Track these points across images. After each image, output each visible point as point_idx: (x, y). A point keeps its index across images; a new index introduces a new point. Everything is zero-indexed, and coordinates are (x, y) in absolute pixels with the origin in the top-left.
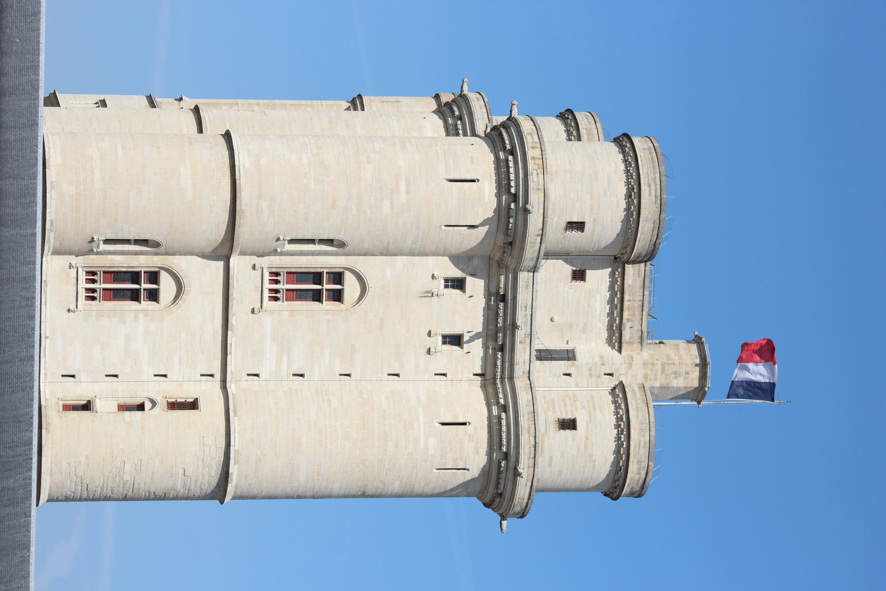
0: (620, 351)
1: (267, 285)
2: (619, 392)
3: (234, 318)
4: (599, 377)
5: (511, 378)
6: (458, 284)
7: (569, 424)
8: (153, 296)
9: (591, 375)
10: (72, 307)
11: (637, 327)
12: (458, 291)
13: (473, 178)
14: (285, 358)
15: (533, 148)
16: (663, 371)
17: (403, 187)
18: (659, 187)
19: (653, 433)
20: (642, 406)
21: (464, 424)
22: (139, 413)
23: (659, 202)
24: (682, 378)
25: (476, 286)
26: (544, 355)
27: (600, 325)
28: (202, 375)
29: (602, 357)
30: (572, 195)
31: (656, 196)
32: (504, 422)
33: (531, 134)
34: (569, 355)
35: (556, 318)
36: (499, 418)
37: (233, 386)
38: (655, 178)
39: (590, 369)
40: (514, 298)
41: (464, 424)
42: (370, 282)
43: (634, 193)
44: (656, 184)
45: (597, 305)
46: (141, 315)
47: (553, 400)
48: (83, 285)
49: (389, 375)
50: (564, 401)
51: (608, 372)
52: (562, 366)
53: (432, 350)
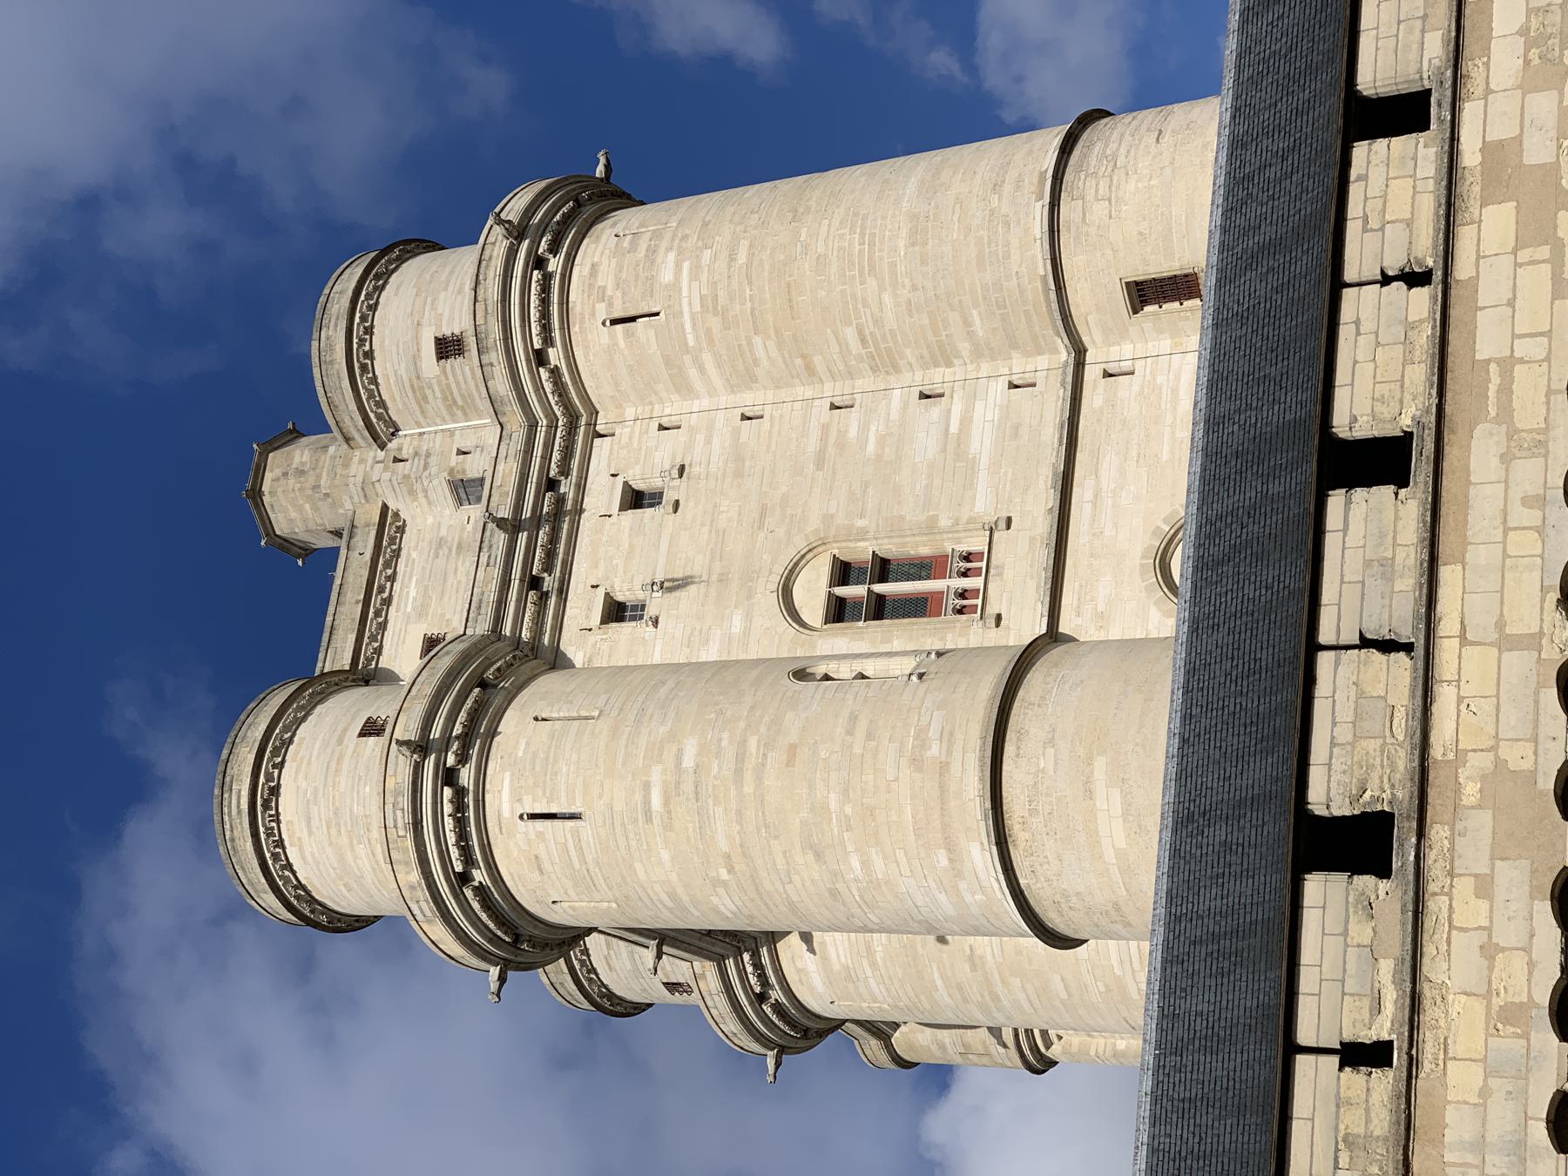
0: (385, 508)
2: (381, 430)
4: (416, 454)
5: (533, 426)
6: (616, 612)
7: (447, 348)
9: (428, 455)
11: (354, 555)
12: (620, 598)
14: (954, 428)
15: (412, 888)
18: (226, 810)
19: (315, 344)
20: (336, 399)
21: (614, 322)
23: (228, 779)
25: (583, 608)
27: (414, 555)
29: (412, 492)
37: (1064, 356)
39: (426, 467)
41: (614, 322)
42: (769, 600)
43: (265, 799)
45: (413, 593)
52: (475, 467)
53: (675, 473)
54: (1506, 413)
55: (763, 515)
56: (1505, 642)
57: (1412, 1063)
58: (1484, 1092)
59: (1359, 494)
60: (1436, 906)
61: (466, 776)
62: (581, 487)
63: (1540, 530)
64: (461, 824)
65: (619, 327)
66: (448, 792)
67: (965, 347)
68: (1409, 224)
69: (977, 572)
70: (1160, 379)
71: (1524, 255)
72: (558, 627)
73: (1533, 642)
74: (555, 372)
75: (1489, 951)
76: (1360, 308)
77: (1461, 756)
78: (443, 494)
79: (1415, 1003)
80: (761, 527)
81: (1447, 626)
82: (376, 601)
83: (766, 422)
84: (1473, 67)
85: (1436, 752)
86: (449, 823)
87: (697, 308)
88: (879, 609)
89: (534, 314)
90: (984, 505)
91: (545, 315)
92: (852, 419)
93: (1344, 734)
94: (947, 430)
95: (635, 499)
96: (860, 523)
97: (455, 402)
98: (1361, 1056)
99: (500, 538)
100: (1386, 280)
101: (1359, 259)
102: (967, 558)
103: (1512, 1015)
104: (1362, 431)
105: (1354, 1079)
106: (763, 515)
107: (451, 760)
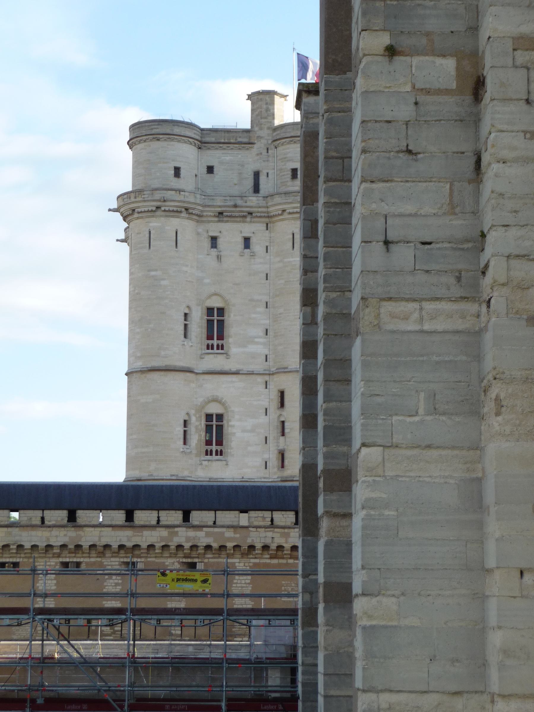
1: (215, 351)
3: (232, 370)
4: (268, 156)
8: (220, 417)
9: (268, 161)
10: (224, 463)
12: (218, 240)
13: (148, 232)
14: (256, 340)
15: (130, 198)
16: (266, 118)
18: (153, 123)
21: (293, 234)
22: (286, 424)
23: (161, 123)
24: (270, 107)
26: (256, 189)
27: (240, 156)
28: (266, 388)
29: (258, 155)
30: (158, 174)
31: (158, 125)
32: (291, 211)
33: (123, 200)
34: (257, 175)
35: (236, 182)
36: (290, 213)
37: (272, 370)
38: (149, 126)
40: (220, 207)
41: (293, 234)
44: (152, 125)
45: (228, 158)
46: (230, 423)
47: (281, 183)
48: (214, 457)
49: (267, 279)
50: (281, 176)
51: (266, 151)
52: (263, 179)
53: (252, 254)
54: (135, 536)
55: (237, 284)
56: (100, 537)
57: (41, 527)
59: (125, 515)
60: (63, 529)
61: (159, 213)
63: (116, 541)
65: (291, 236)
66: (154, 209)
68: (167, 520)
69: (218, 349)
70: (263, 396)
71: (159, 538)
72: (209, 222)
73: (100, 540)
75: (57, 536)
76: (154, 514)
77: (84, 531)
78: (256, 166)
79: (49, 527)
80: (234, 284)
81: (103, 529)
82: (225, 146)
83: (265, 281)
84: (191, 529)
86: (146, 209)
88: (210, 323)
90: (234, 350)
92: (262, 309)
93: (88, 515)
94: (256, 338)
96: (232, 315)
97: (281, 173)
98: (43, 519)
99: (232, 203)
100: (158, 517)
101: (163, 513)
102: (222, 346)
103: (48, 539)
104: (135, 515)
105: (39, 519)
106: (237, 284)
107: (163, 209)
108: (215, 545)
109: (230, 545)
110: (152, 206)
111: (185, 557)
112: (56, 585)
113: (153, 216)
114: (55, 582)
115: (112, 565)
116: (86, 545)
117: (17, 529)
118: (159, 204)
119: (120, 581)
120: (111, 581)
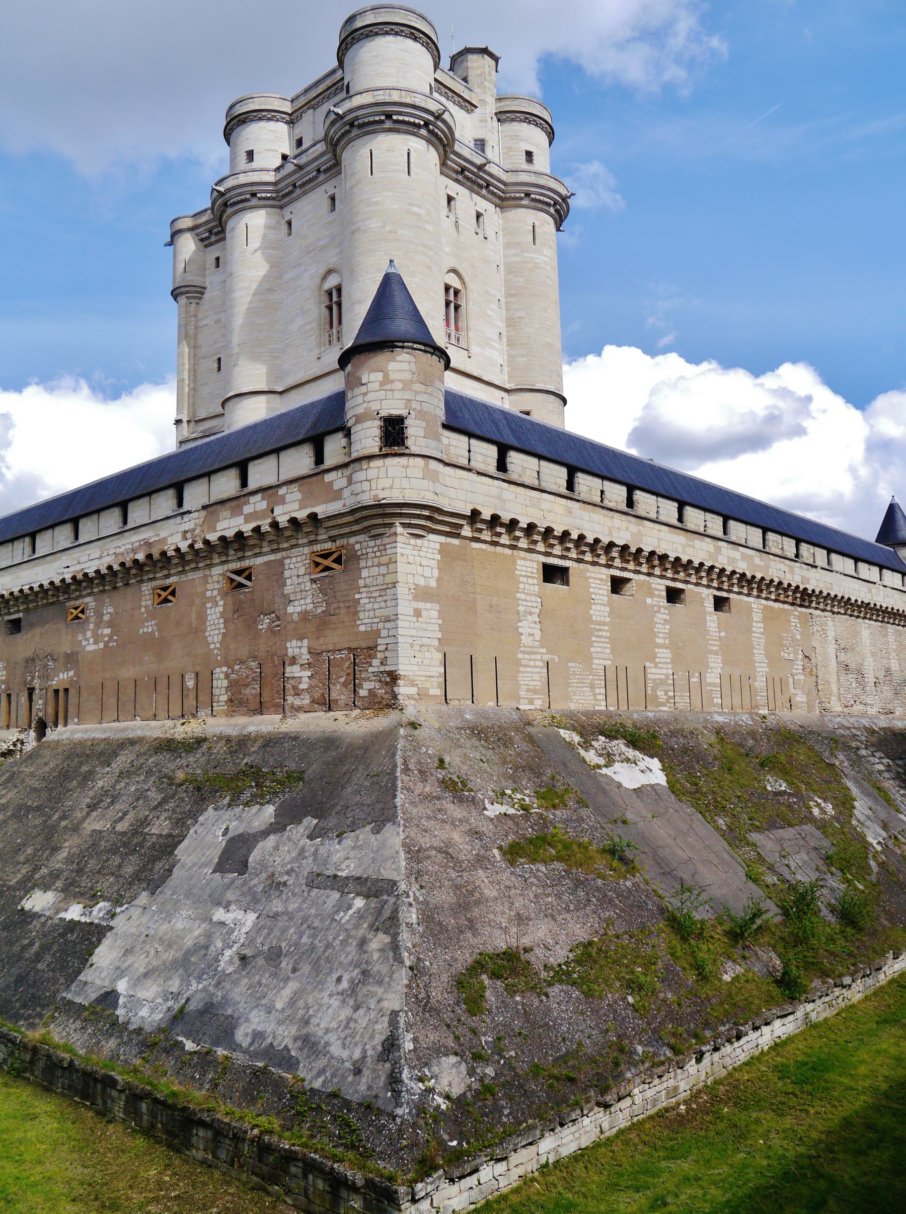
0: (476, 107)
5: (505, 184)
7: (529, 154)
14: (492, 343)
15: (390, 96)
17: (415, 209)
25: (454, 189)
29: (481, 121)
32: (538, 197)
40: (466, 160)
56: (659, 539)
57: (603, 508)
58: (600, 524)
62: (483, 197)
64: (409, 123)
66: (422, 123)
67: (514, 352)
73: (659, 547)
74: (521, 199)
75: (619, 529)
79: (611, 510)
82: (450, 94)
85: (645, 522)
86: (412, 120)
87: (536, 260)
88: (448, 304)
89: (542, 198)
90: (474, 349)
91: (539, 201)
92: (494, 307)
95: (479, 216)
96: (471, 303)
103: (611, 534)
108: (749, 575)
109: (759, 576)
110: (420, 118)
111: (719, 589)
112: (611, 613)
113: (414, 134)
114: (608, 609)
115: (657, 590)
116: (647, 549)
117: (577, 505)
118: (431, 118)
119: (668, 618)
120: (660, 616)
